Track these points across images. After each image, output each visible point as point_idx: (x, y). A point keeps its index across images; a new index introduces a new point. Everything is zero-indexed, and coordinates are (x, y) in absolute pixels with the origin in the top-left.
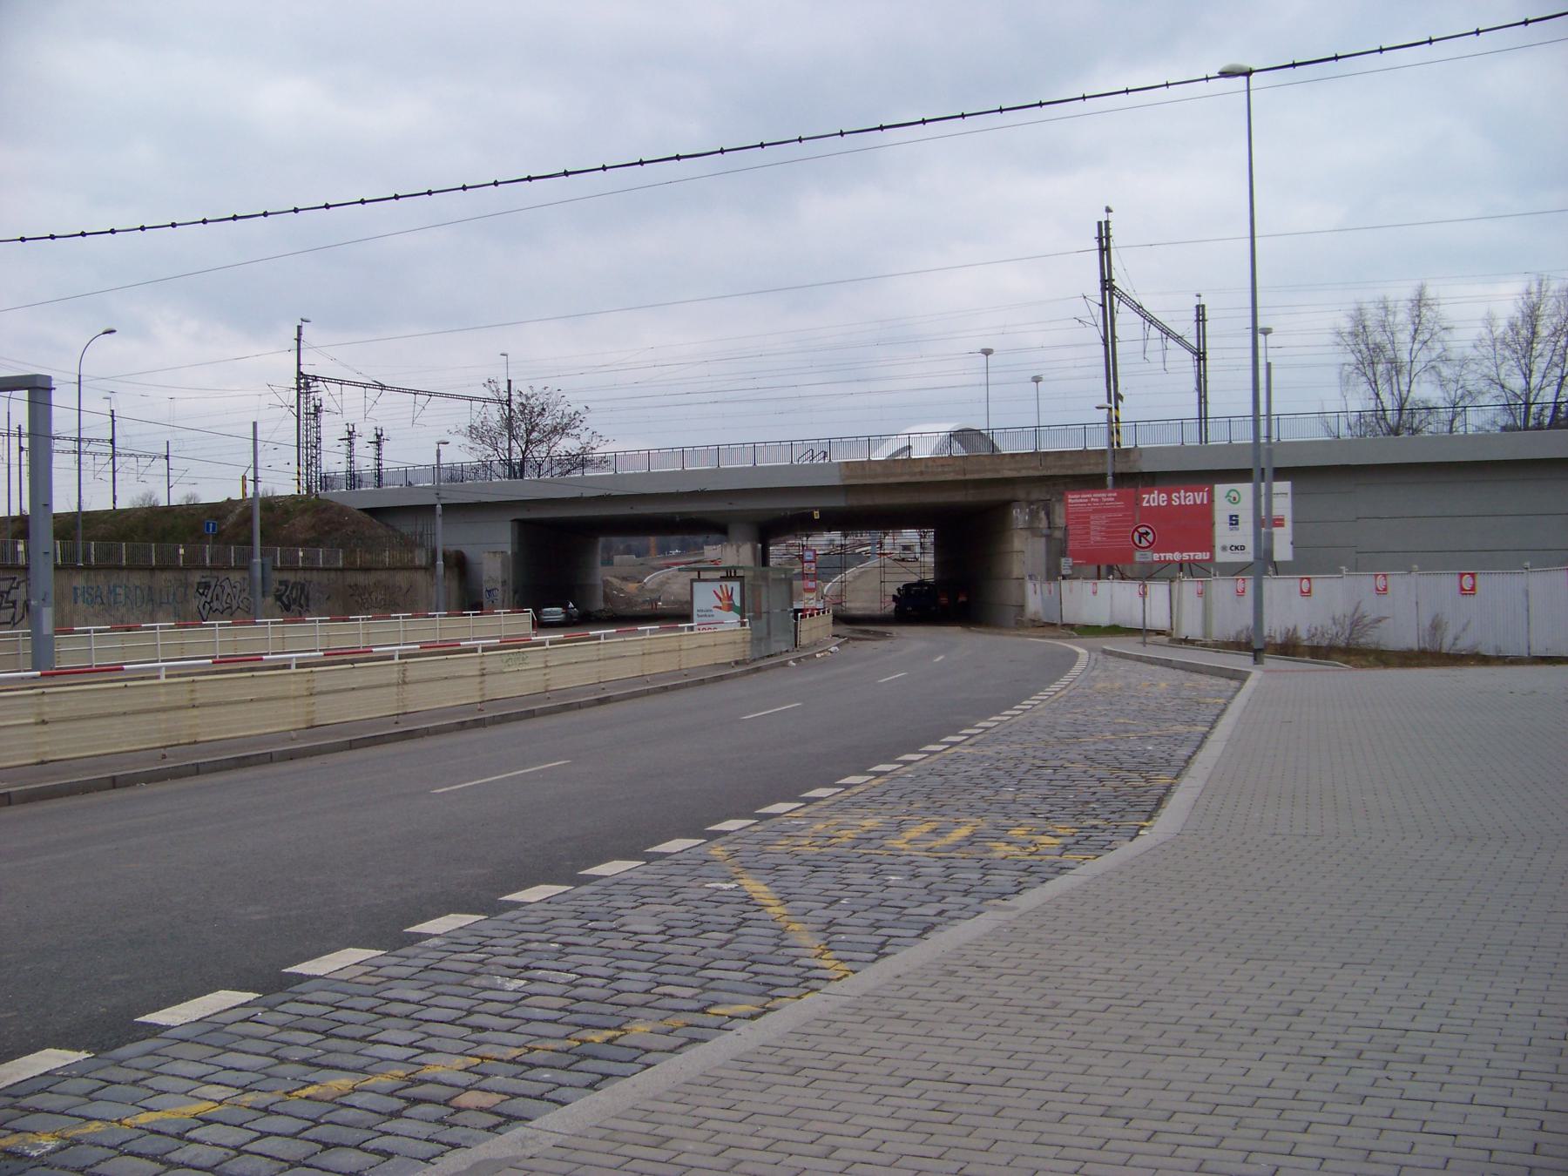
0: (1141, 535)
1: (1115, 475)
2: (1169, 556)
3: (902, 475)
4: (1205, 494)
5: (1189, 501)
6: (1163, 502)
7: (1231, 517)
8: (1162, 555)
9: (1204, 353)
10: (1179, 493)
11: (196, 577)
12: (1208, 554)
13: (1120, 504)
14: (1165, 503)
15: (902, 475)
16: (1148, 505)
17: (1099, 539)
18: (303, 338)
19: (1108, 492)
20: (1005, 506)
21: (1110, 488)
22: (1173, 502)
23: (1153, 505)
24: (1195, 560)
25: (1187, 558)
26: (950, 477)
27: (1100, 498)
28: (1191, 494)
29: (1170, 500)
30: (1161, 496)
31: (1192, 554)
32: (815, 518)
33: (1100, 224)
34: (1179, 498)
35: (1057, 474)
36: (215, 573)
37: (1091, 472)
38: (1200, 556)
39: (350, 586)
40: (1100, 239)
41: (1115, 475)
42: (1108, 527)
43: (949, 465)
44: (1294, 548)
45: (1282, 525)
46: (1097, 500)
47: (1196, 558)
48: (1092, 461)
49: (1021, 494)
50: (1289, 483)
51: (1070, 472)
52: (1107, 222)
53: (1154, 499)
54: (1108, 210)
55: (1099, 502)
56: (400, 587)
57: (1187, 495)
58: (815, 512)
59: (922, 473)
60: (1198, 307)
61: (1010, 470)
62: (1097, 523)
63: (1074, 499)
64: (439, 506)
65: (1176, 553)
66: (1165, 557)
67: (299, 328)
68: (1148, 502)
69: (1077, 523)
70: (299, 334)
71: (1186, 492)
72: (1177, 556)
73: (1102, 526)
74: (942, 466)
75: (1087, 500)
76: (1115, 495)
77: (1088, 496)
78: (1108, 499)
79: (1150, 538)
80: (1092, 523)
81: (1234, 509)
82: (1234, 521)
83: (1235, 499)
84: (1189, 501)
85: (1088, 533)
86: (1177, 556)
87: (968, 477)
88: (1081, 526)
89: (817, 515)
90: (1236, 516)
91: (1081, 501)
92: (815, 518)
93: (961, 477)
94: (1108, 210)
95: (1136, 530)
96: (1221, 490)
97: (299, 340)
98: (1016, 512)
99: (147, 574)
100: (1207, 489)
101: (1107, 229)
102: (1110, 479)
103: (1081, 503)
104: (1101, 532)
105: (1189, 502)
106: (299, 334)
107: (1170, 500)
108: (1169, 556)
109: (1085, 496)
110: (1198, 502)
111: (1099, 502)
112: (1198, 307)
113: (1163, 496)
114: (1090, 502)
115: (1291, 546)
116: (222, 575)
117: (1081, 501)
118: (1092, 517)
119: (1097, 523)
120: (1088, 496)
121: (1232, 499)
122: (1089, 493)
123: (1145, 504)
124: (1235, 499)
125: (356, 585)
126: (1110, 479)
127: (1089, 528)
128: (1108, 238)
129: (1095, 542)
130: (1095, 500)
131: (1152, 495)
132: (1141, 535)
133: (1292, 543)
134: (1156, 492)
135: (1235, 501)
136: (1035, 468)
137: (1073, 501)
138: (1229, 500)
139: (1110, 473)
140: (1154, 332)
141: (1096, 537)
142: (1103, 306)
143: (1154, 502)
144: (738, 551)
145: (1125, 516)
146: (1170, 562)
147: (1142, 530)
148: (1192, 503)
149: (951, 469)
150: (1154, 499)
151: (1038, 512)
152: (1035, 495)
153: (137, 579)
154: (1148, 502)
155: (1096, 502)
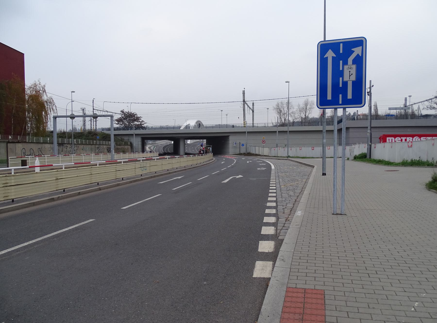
0: (263, 142)
1: (247, 132)
9: (254, 111)
11: (97, 146)
18: (94, 102)
33: (243, 91)
36: (99, 146)
39: (117, 148)
40: (243, 93)
41: (247, 132)
52: (244, 91)
54: (244, 88)
56: (126, 148)
60: (253, 103)
64: (134, 135)
67: (93, 100)
70: (93, 101)
79: (265, 142)
94: (244, 88)
95: (263, 141)
97: (93, 102)
99: (91, 145)
101: (244, 92)
102: (247, 132)
106: (93, 101)
112: (253, 103)
116: (100, 146)
125: (118, 148)
126: (247, 132)
128: (244, 93)
132: (263, 142)
140: (249, 108)
142: (243, 104)
147: (264, 141)
153: (90, 146)
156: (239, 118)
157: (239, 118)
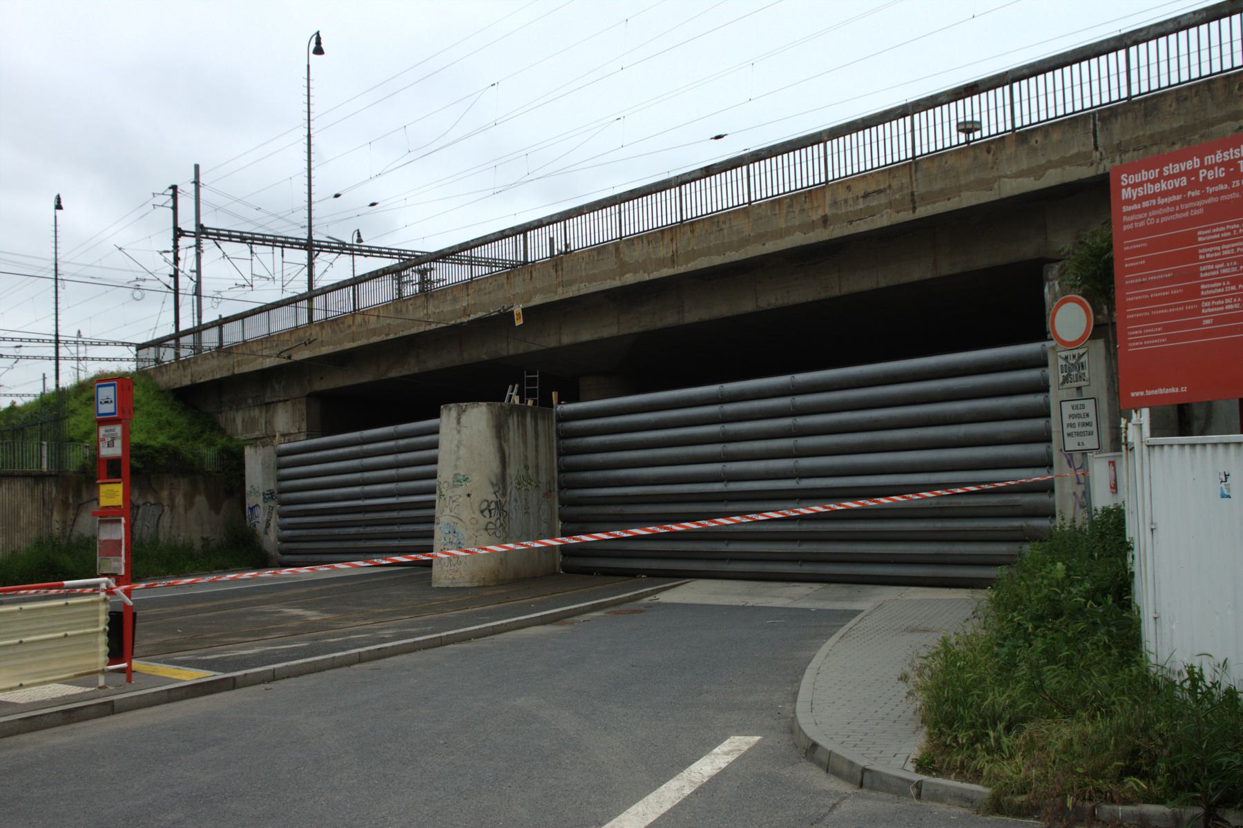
3: (788, 232)
15: (788, 232)
26: (885, 220)
43: (879, 192)
46: (1221, 173)
49: (1062, 241)
59: (825, 221)
61: (1020, 175)
69: (1152, 264)
74: (866, 196)
75: (1184, 181)
77: (1188, 165)
80: (1206, 253)
85: (1195, 292)
87: (923, 211)
88: (1166, 272)
91: (1163, 186)
93: (906, 216)
111: (1227, 180)
114: (1191, 186)
117: (1163, 186)
120: (1188, 165)
127: (1195, 274)
129: (1217, 320)
136: (1074, 160)
137: (1140, 191)
144: (459, 422)
149: (883, 199)
155: (1217, 181)
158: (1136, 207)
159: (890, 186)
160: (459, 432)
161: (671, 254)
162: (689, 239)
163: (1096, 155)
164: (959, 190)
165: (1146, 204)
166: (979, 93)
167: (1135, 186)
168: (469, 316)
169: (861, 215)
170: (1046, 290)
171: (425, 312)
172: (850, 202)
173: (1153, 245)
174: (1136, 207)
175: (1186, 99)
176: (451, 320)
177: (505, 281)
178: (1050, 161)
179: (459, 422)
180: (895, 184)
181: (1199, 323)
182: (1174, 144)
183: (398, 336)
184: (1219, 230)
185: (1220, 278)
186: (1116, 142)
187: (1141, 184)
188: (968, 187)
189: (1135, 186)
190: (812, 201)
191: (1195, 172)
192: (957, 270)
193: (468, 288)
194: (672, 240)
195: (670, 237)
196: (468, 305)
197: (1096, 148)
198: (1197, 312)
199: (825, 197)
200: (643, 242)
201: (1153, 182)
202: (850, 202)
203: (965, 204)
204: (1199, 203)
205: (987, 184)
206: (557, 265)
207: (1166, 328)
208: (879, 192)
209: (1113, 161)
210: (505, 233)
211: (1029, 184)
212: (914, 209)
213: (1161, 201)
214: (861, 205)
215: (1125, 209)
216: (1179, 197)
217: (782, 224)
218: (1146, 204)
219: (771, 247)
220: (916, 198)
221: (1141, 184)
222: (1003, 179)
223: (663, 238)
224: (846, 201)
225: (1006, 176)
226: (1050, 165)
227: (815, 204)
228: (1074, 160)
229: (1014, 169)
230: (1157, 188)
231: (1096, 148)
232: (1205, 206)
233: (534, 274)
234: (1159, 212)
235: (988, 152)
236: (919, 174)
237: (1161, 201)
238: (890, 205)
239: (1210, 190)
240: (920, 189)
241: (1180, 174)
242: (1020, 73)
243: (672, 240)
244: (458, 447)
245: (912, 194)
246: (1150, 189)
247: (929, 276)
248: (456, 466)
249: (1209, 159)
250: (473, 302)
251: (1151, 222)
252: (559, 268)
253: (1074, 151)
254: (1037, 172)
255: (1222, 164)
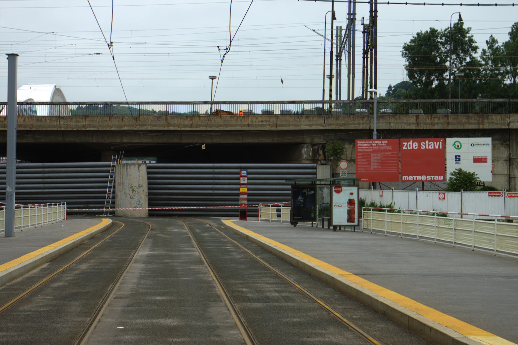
1: (378, 131)
2: (419, 178)
4: (441, 143)
5: (431, 147)
6: (415, 147)
7: (456, 157)
8: (415, 177)
10: (425, 142)
12: (442, 177)
13: (390, 148)
14: (417, 148)
15: (236, 125)
16: (406, 148)
17: (376, 167)
19: (374, 140)
20: (298, 146)
21: (375, 137)
22: (422, 148)
23: (409, 148)
24: (434, 180)
25: (430, 179)
26: (268, 128)
27: (377, 144)
28: (432, 143)
29: (419, 146)
30: (414, 143)
31: (433, 177)
32: (203, 149)
34: (425, 145)
35: (334, 129)
37: (356, 128)
38: (437, 178)
41: (378, 131)
42: (382, 161)
43: (266, 121)
44: (492, 174)
45: (486, 162)
46: (375, 145)
47: (435, 179)
48: (356, 122)
49: (308, 140)
50: (490, 139)
51: (342, 128)
53: (410, 145)
55: (376, 146)
57: (430, 143)
58: (203, 146)
59: (249, 125)
61: (305, 125)
62: (375, 158)
63: (361, 144)
65: (410, 177)
66: (434, 178)
68: (407, 146)
69: (363, 158)
71: (429, 142)
72: (424, 178)
73: (378, 160)
74: (262, 121)
75: (369, 145)
76: (387, 142)
78: (382, 145)
80: (372, 158)
81: (457, 152)
82: (458, 159)
83: (458, 146)
84: (431, 147)
85: (370, 164)
86: (424, 178)
87: (279, 128)
89: (204, 147)
90: (459, 156)
91: (365, 145)
92: (203, 149)
93: (274, 128)
96: (450, 141)
98: (304, 150)
100: (441, 140)
102: (375, 133)
103: (366, 146)
104: (377, 163)
105: (431, 147)
107: (419, 146)
108: (419, 178)
109: (368, 142)
110: (437, 147)
111: (377, 146)
113: (416, 145)
114: (371, 146)
115: (491, 174)
117: (365, 145)
118: (372, 154)
119: (375, 158)
121: (456, 147)
122: (369, 141)
123: (404, 148)
124: (458, 146)
126: (375, 133)
127: (370, 161)
129: (373, 169)
130: (374, 145)
131: (409, 143)
133: (491, 172)
134: (411, 141)
135: (458, 148)
136: (319, 125)
137: (361, 145)
138: (455, 147)
139: (375, 130)
141: (374, 166)
143: (410, 147)
144: (139, 169)
145: (391, 154)
146: (417, 181)
148: (433, 148)
149: (267, 123)
150: (410, 145)
151: (318, 151)
152: (317, 140)
154: (407, 146)
155: (375, 146)
156: (282, 81)
157: (282, 81)
158: (360, 147)
159: (270, 121)
160: (139, 172)
161: (190, 124)
162: (198, 121)
163: (324, 125)
164: (289, 126)
165: (362, 147)
166: (295, 103)
167: (360, 144)
168: (86, 128)
169: (260, 126)
170: (303, 150)
171: (58, 123)
172: (257, 122)
173: (363, 155)
174: (360, 147)
175: (345, 118)
176: (74, 128)
177: (109, 119)
178: (313, 124)
179: (139, 169)
180: (271, 120)
181: (371, 169)
182: (342, 126)
183: (38, 129)
184: (375, 154)
185: (375, 162)
186: (329, 123)
187: (361, 144)
188: (292, 125)
189: (360, 144)
190: (244, 119)
191: (371, 144)
192: (279, 142)
193: (86, 119)
194: (191, 120)
195: (190, 119)
196: (86, 125)
197: (325, 123)
198: (370, 167)
199: (249, 119)
200: (178, 118)
201: (364, 144)
202: (257, 122)
203: (291, 129)
204: (372, 149)
205: (298, 126)
206: (136, 118)
207: (365, 169)
208: (266, 121)
209: (328, 127)
210: (107, 103)
211: (308, 128)
212: (276, 127)
213: (365, 147)
214: (260, 123)
215: (358, 147)
216: (368, 147)
217: (234, 123)
218: (362, 147)
219: (229, 128)
220: (277, 125)
221: (361, 144)
222: (302, 126)
223: (187, 119)
224: (256, 121)
225: (302, 125)
226: (313, 125)
227: (246, 120)
228: (319, 125)
229: (304, 124)
230: (364, 145)
231: (325, 123)
232: (373, 150)
233: (124, 120)
234: (365, 149)
235: (298, 118)
236: (279, 119)
237: (365, 147)
238: (269, 125)
239: (373, 147)
240: (279, 123)
241: (368, 144)
242: (306, 102)
243: (191, 120)
244: (139, 176)
245: (276, 124)
246: (363, 145)
247: (271, 142)
248: (139, 182)
249: (373, 142)
250: (89, 124)
251: (363, 151)
252: (138, 120)
253: (320, 123)
254: (310, 126)
255: (376, 143)
